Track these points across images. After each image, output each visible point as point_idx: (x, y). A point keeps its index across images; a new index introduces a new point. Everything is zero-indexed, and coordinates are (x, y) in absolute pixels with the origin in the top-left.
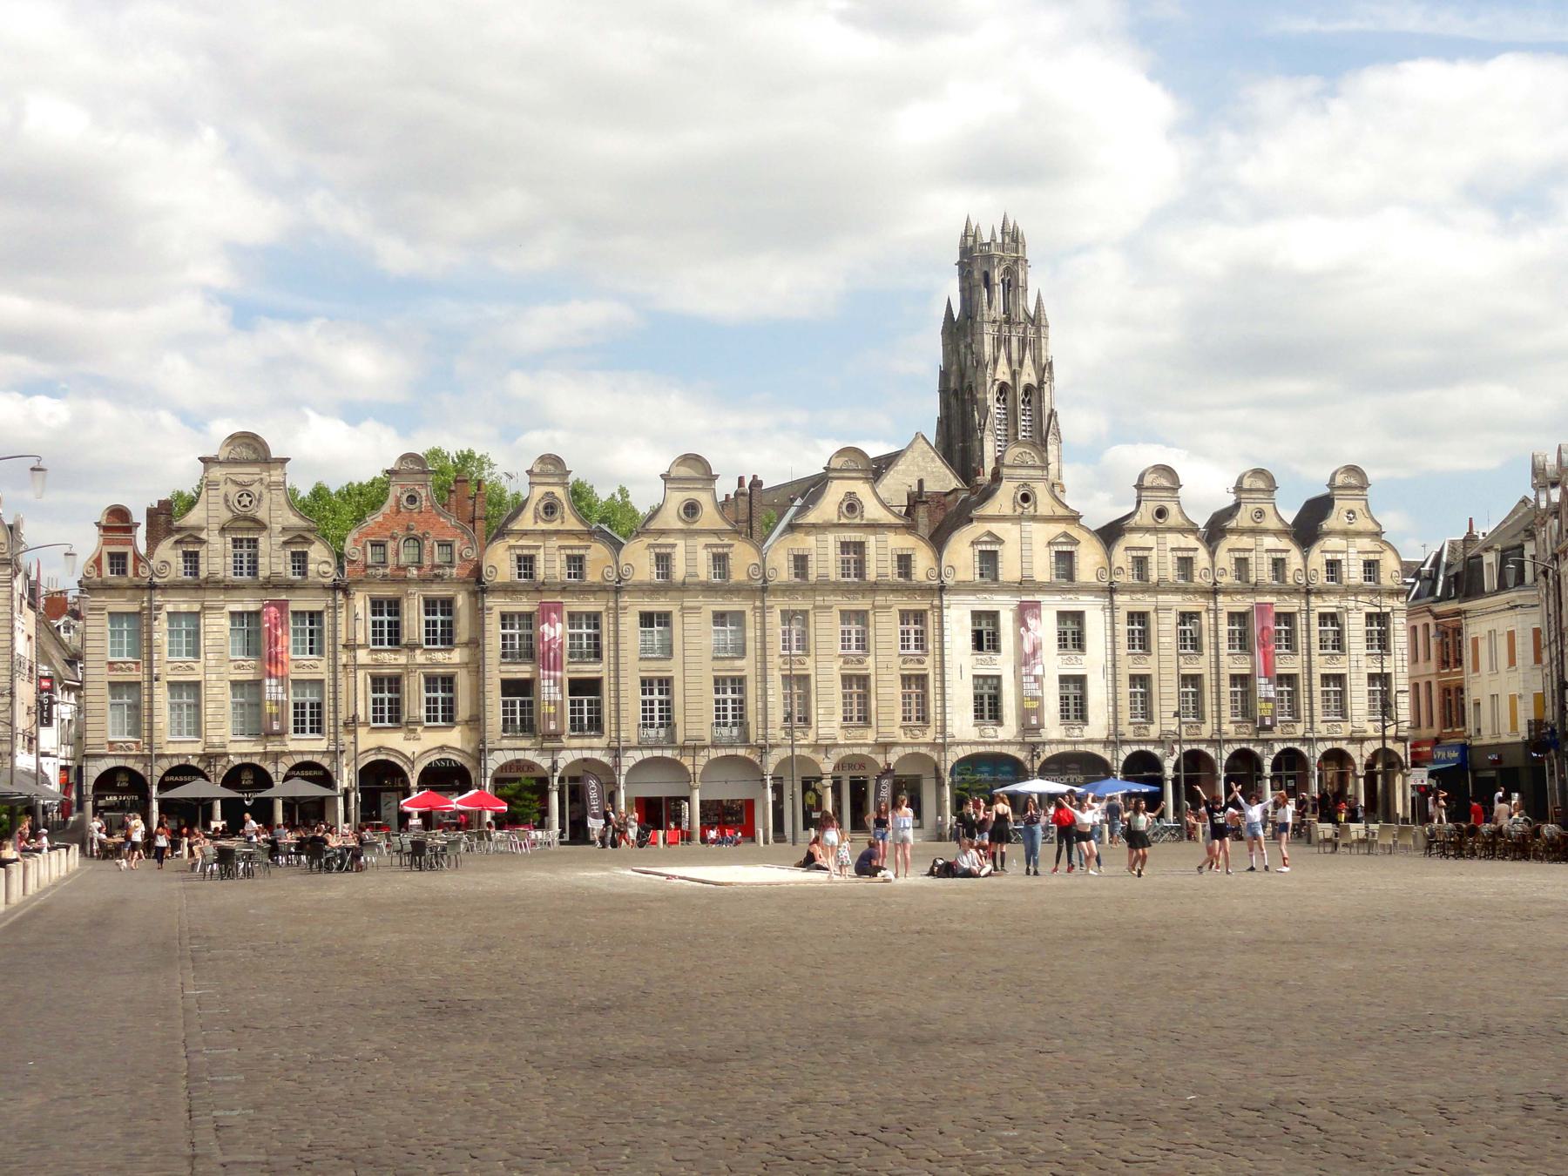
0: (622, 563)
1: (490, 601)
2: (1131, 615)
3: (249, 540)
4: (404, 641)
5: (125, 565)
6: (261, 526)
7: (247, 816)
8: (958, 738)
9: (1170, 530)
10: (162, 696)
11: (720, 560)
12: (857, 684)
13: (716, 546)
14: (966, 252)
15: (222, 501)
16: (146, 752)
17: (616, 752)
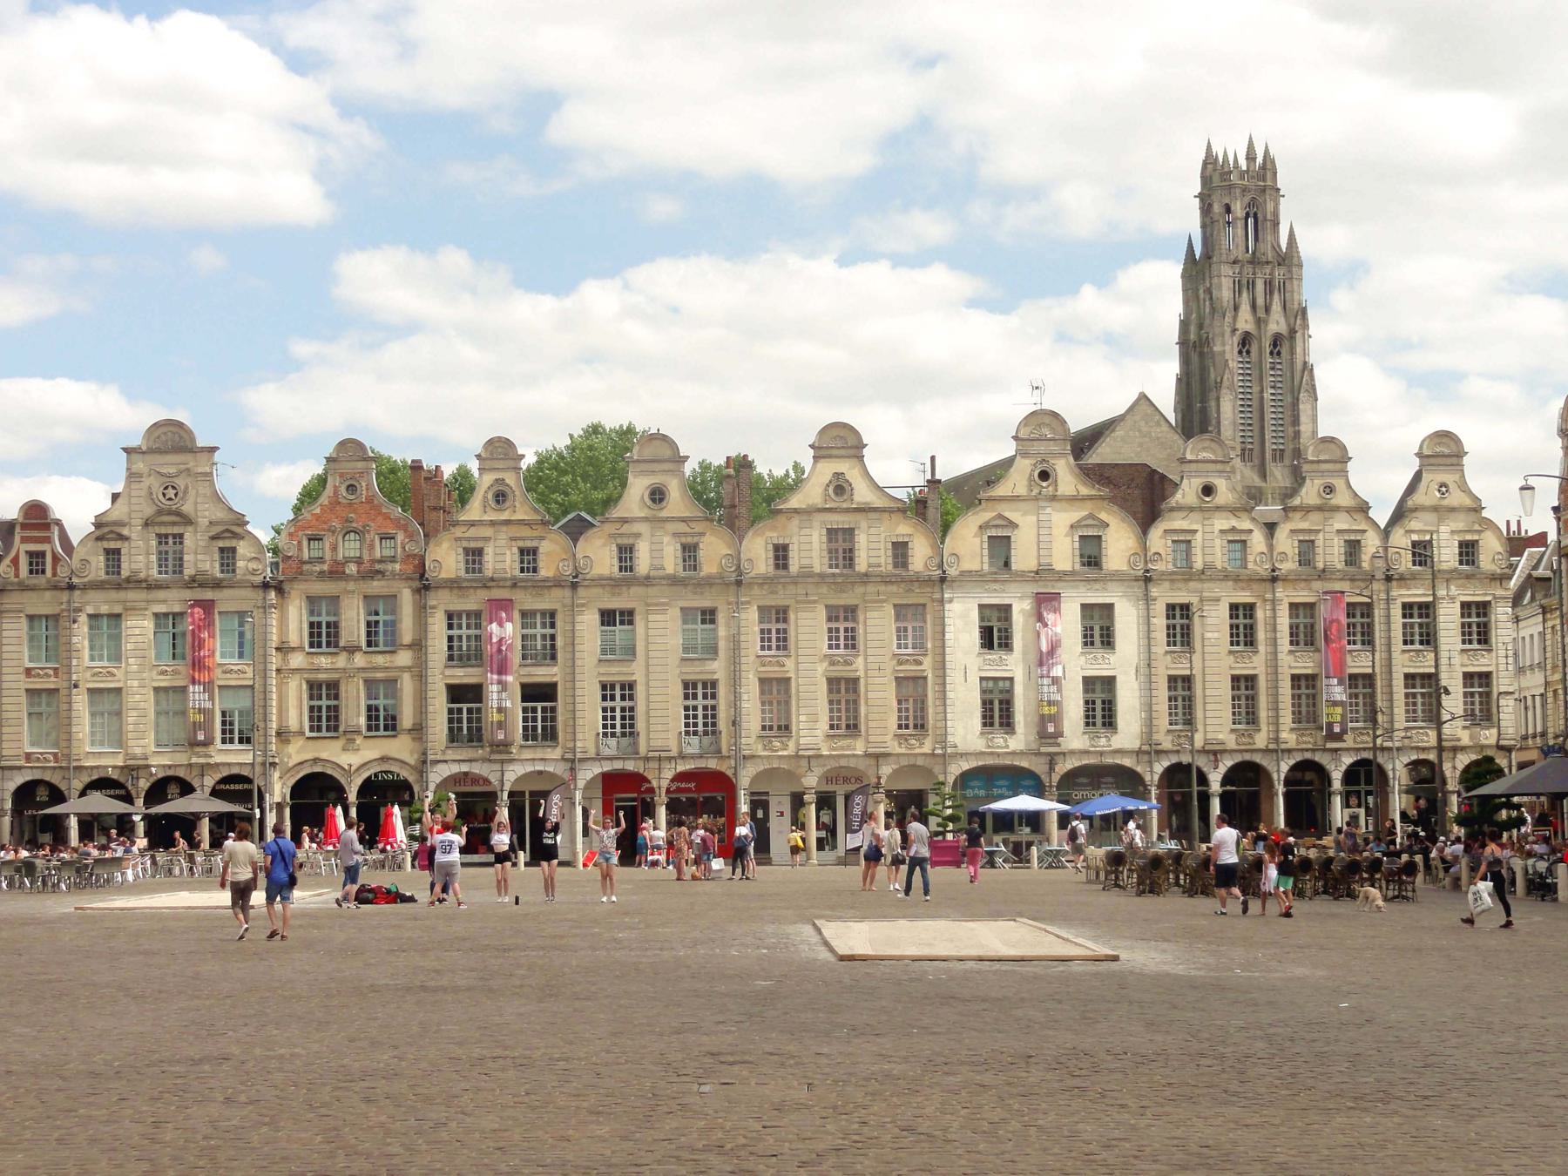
0: (579, 556)
1: (433, 599)
2: (1171, 608)
3: (174, 536)
4: (342, 644)
5: (44, 564)
6: (188, 521)
7: (177, 834)
8: (961, 749)
9: (1218, 508)
10: (81, 702)
11: (690, 552)
12: (844, 690)
13: (686, 534)
14: (1206, 180)
17: (572, 763)
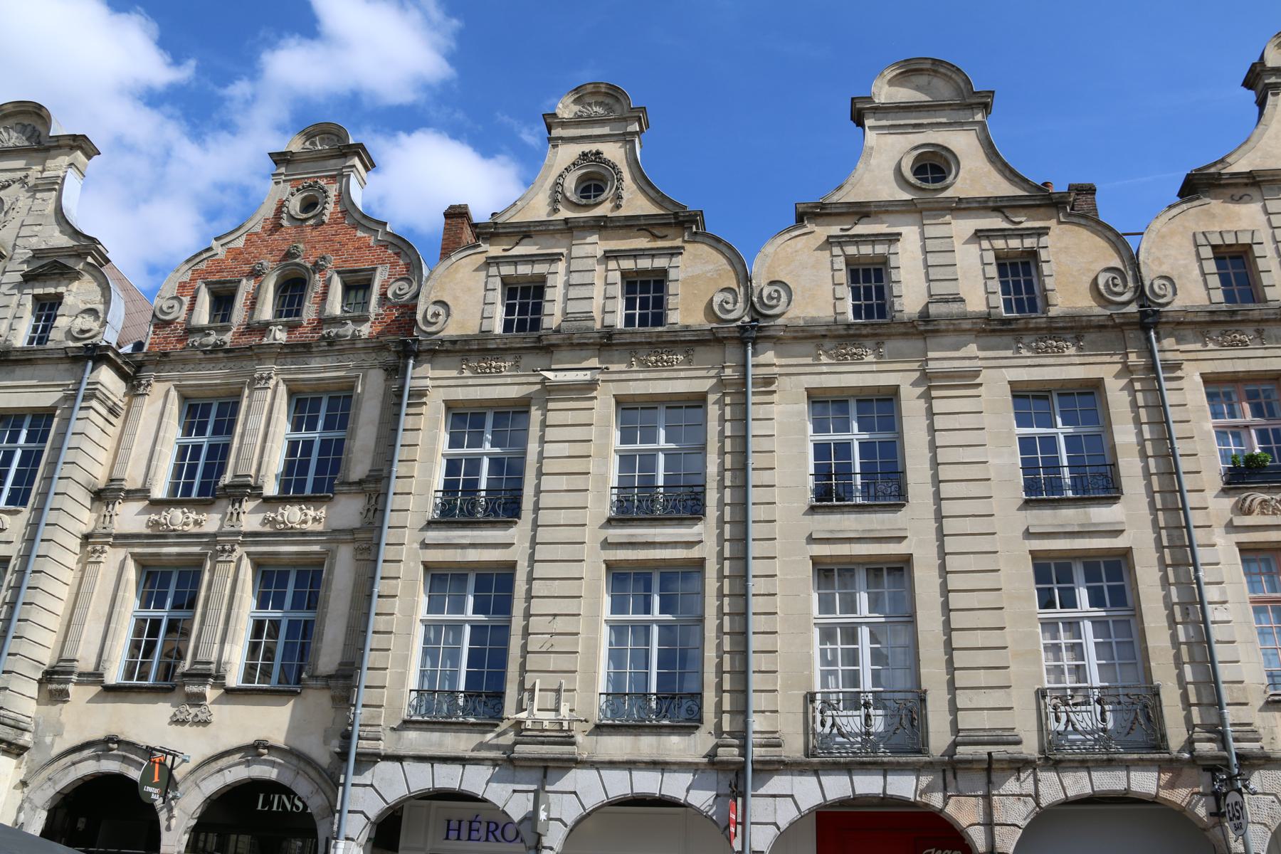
0: (760, 279)
1: (421, 375)
17: (734, 776)
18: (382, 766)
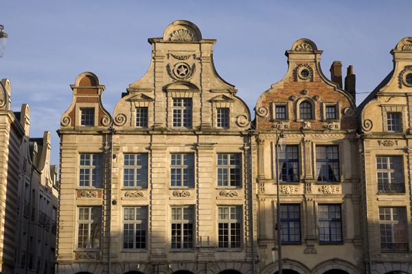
3: (185, 99)
15: (165, 70)
16: (105, 260)
18: (378, 265)
